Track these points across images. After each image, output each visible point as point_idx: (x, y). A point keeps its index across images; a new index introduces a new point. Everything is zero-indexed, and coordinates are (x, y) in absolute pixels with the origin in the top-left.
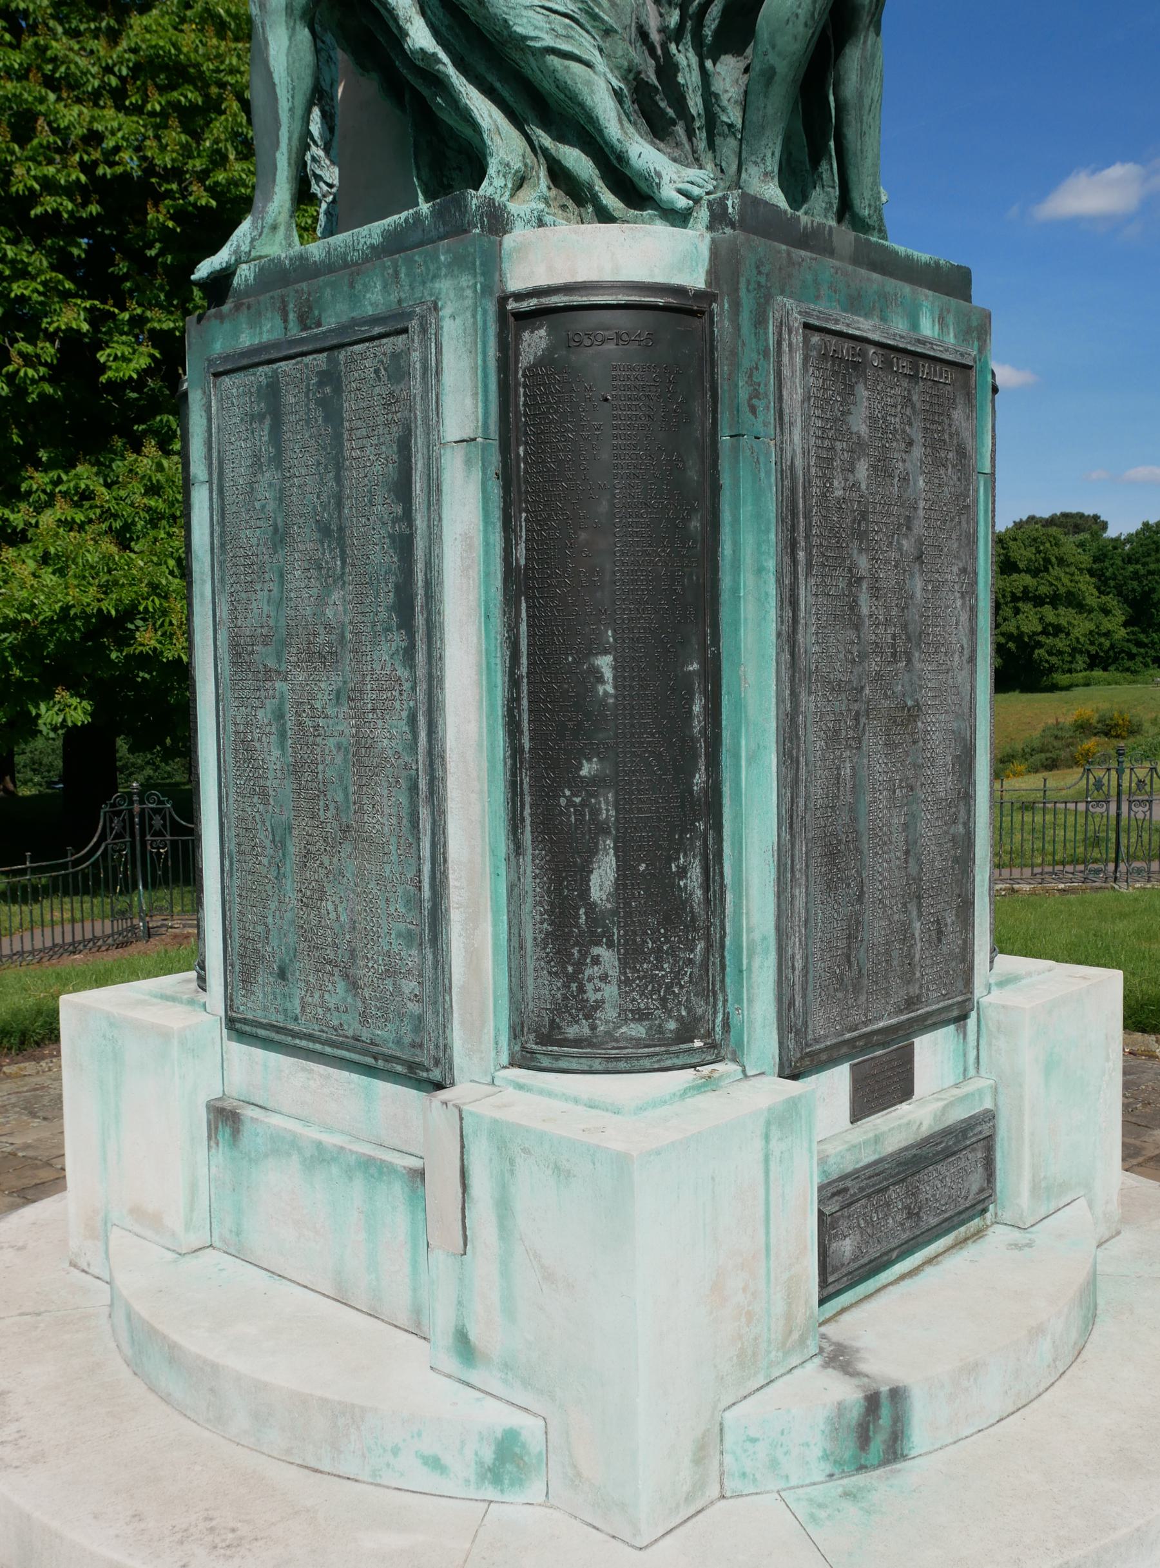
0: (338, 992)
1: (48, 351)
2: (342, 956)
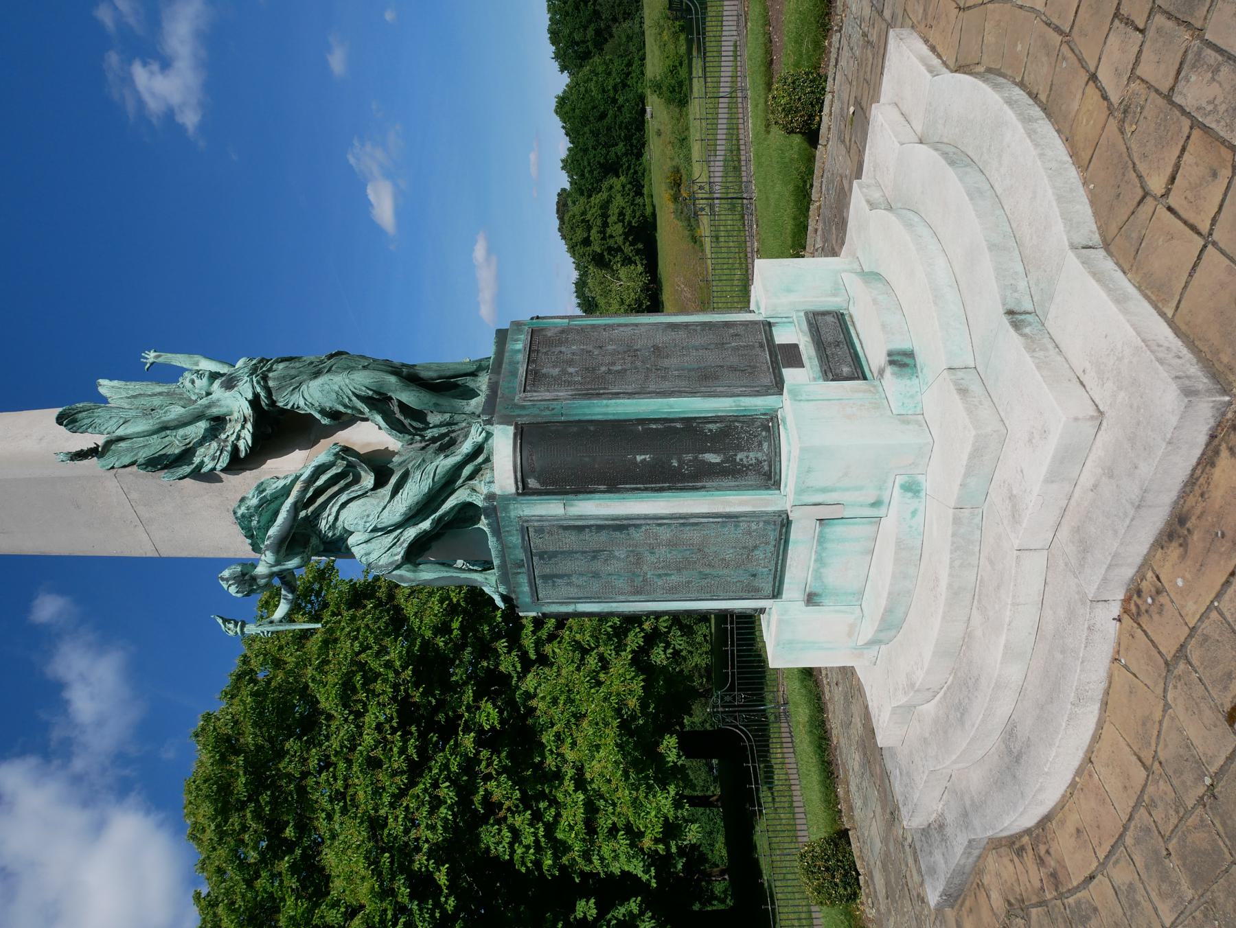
0: (759, 553)
1: (485, 753)
2: (745, 552)
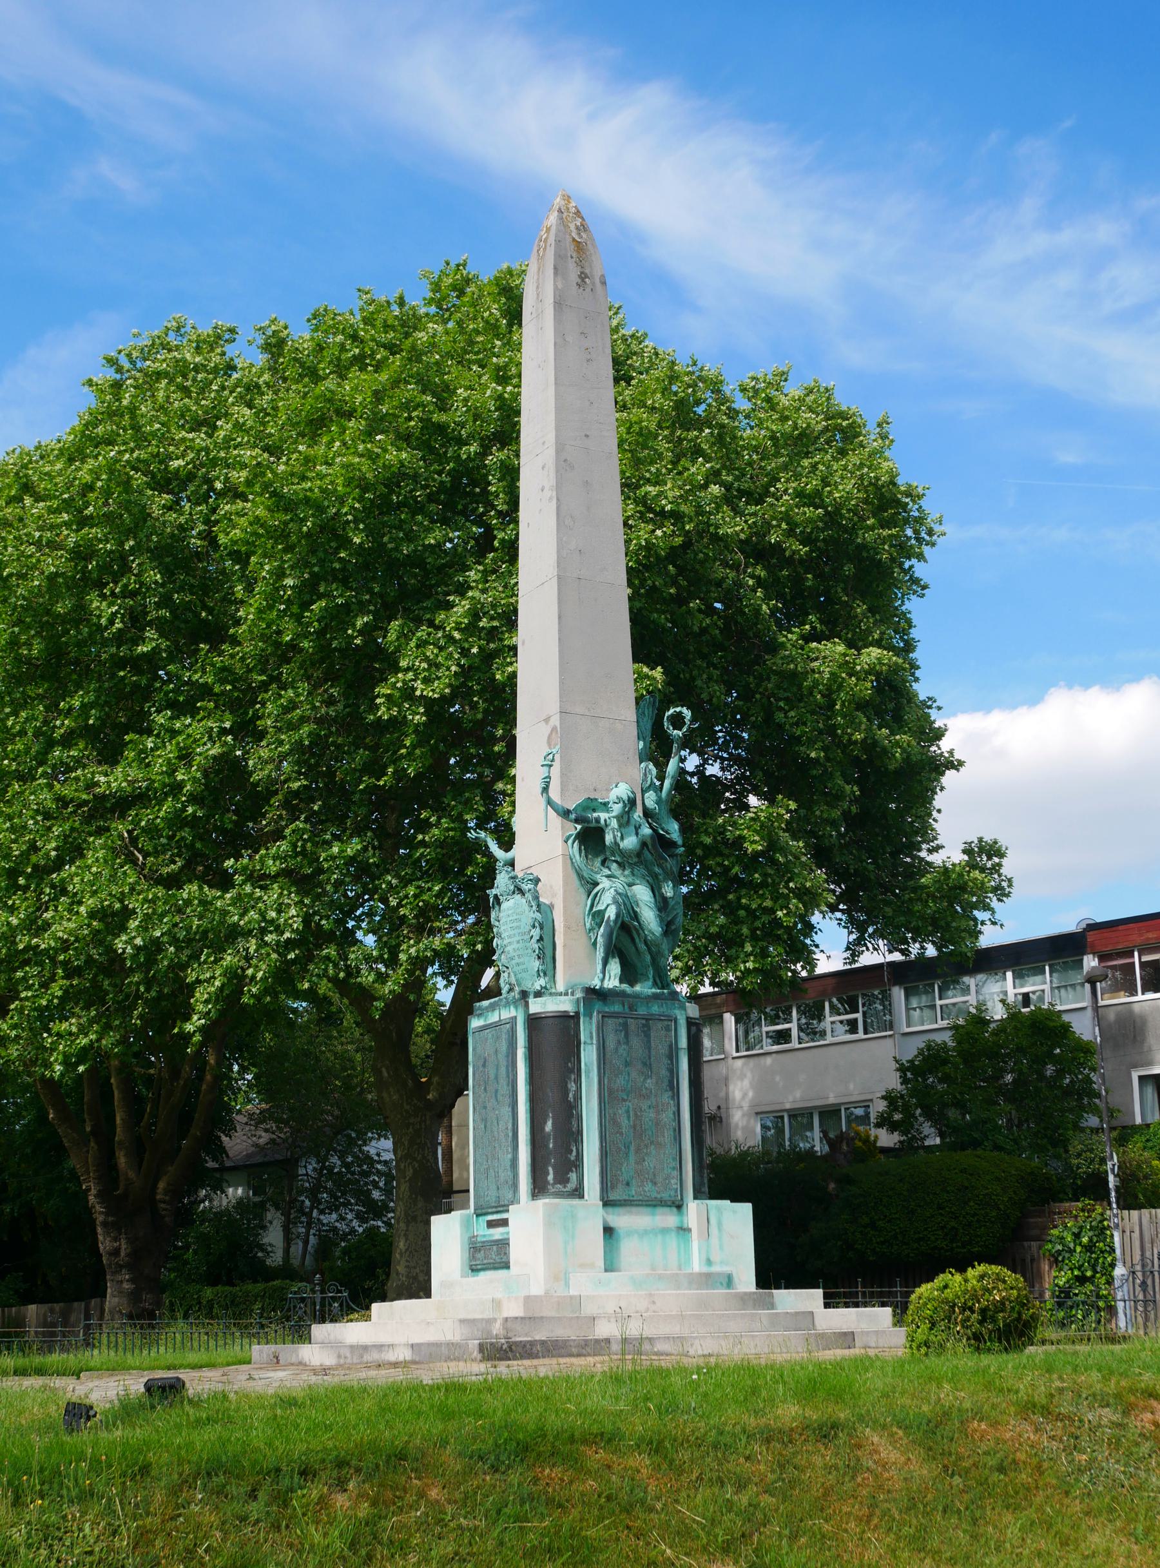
0: (649, 1187)
